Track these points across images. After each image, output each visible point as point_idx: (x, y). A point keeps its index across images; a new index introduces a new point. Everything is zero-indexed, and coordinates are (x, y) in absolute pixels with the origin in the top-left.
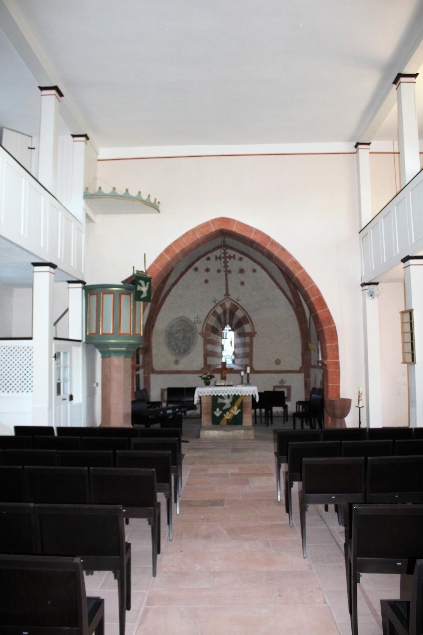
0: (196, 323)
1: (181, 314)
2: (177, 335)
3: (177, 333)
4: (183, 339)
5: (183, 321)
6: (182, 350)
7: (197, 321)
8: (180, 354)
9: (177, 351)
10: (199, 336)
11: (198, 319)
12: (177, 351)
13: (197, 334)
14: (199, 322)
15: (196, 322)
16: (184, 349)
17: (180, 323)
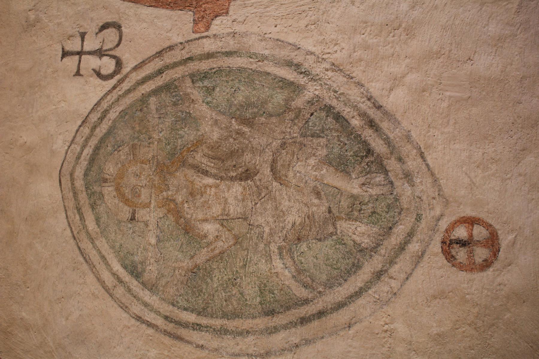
0: (119, 63)
1: (46, 191)
2: (210, 228)
3: (187, 229)
4: (247, 175)
5: (94, 177)
6: (354, 187)
7: (100, 53)
8: (386, 212)
9: (359, 231)
10: (219, 25)
11: (91, 44)
12: (359, 231)
13: (209, 46)
14: (111, 34)
15: (107, 65)
16: (341, 165)
17: (109, 190)
